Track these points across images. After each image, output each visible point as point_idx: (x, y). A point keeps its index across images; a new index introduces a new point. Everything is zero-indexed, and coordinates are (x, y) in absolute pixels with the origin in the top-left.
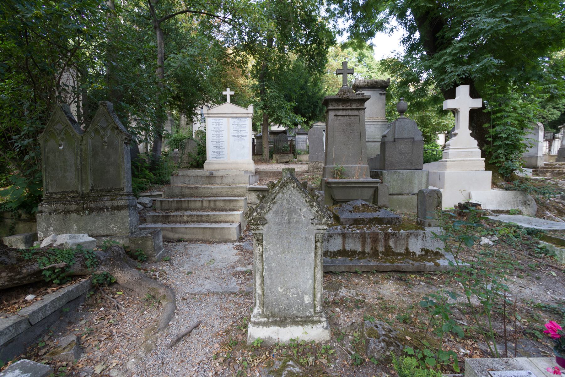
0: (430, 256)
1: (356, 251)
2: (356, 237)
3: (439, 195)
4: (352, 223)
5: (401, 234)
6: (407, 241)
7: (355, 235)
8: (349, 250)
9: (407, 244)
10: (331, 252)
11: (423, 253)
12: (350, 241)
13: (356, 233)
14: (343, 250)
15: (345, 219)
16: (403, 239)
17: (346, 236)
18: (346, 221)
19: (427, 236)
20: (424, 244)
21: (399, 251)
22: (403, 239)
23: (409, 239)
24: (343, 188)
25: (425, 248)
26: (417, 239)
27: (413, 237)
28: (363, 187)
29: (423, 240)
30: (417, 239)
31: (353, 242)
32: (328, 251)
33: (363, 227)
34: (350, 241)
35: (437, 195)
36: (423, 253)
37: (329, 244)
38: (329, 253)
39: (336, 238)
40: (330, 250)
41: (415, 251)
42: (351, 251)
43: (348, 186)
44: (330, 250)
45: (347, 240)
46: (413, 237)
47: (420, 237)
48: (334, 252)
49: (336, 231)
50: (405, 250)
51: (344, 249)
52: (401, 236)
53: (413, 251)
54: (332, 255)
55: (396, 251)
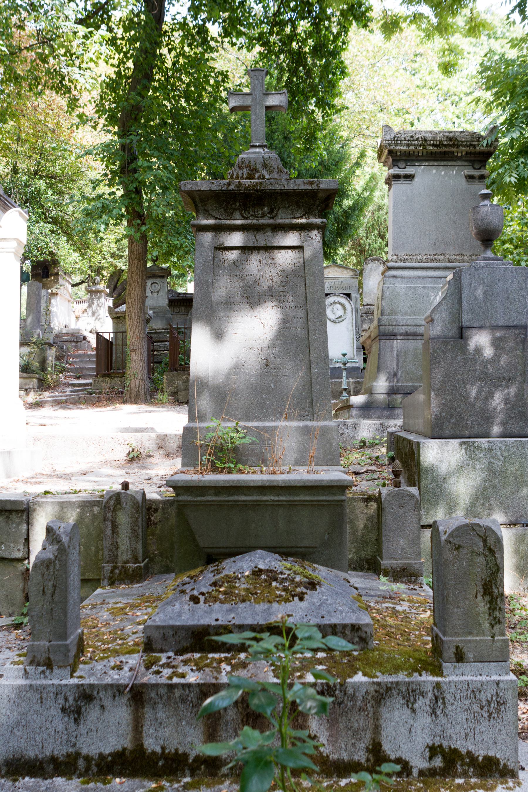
0: (465, 774)
1: (185, 756)
2: (183, 700)
3: (491, 541)
4: (185, 644)
5: (350, 691)
6: (377, 717)
7: (177, 693)
8: (158, 750)
9: (377, 728)
10: (87, 759)
11: (438, 762)
12: (161, 714)
13: (183, 686)
14: (132, 752)
15: (158, 627)
16: (360, 709)
17: (146, 697)
18: (164, 638)
19: (448, 698)
20: (438, 730)
21: (345, 756)
22: (360, 709)
23: (383, 710)
24: (221, 505)
25: (445, 744)
26: (414, 711)
27: (398, 702)
28: (292, 505)
29: (434, 712)
30: (414, 711)
31: (173, 720)
32: (78, 754)
33: (220, 661)
34: (161, 714)
35: (485, 541)
36: (438, 762)
37: (83, 729)
38: (81, 763)
39: (108, 703)
40: (84, 751)
41: (407, 757)
42: (164, 755)
43: (235, 498)
44: (84, 752)
45: (148, 713)
46: (398, 702)
47: (422, 703)
48: (101, 756)
49: (114, 677)
50: (368, 750)
51: (139, 749)
52: (353, 697)
53: (398, 754)
54: (95, 769)
55: (333, 757)
